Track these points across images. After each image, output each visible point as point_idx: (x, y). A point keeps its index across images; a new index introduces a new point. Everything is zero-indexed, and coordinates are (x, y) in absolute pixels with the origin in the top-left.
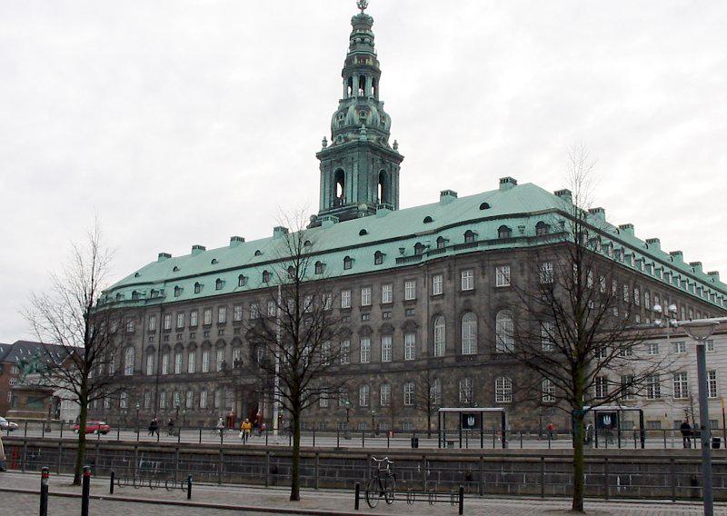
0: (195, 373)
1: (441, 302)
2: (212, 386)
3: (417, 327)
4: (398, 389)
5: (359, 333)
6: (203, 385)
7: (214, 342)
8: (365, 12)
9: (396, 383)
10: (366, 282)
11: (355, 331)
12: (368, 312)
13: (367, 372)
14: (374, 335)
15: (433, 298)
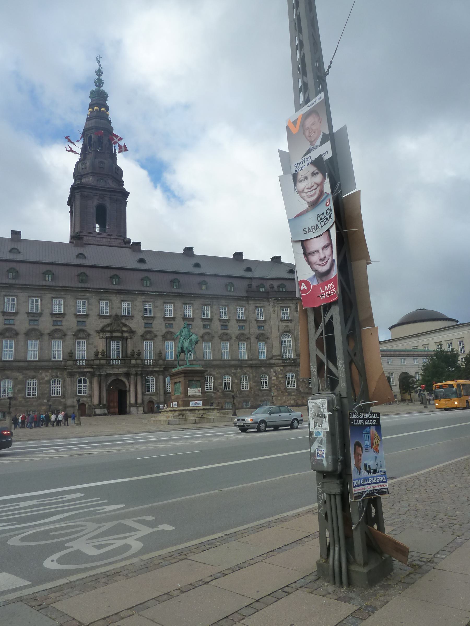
0: (15, 361)
1: (289, 324)
2: (46, 375)
3: (268, 338)
4: (256, 379)
5: (219, 337)
6: (31, 373)
7: (47, 332)
8: (101, 89)
9: (254, 374)
10: (223, 302)
11: (216, 336)
12: (227, 323)
13: (231, 366)
14: (232, 341)
15: (282, 321)
